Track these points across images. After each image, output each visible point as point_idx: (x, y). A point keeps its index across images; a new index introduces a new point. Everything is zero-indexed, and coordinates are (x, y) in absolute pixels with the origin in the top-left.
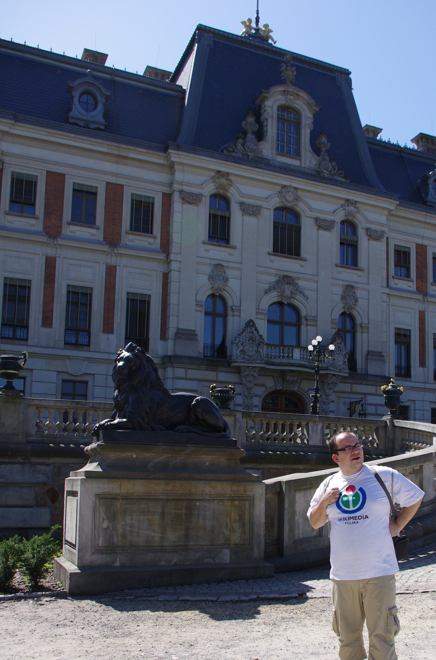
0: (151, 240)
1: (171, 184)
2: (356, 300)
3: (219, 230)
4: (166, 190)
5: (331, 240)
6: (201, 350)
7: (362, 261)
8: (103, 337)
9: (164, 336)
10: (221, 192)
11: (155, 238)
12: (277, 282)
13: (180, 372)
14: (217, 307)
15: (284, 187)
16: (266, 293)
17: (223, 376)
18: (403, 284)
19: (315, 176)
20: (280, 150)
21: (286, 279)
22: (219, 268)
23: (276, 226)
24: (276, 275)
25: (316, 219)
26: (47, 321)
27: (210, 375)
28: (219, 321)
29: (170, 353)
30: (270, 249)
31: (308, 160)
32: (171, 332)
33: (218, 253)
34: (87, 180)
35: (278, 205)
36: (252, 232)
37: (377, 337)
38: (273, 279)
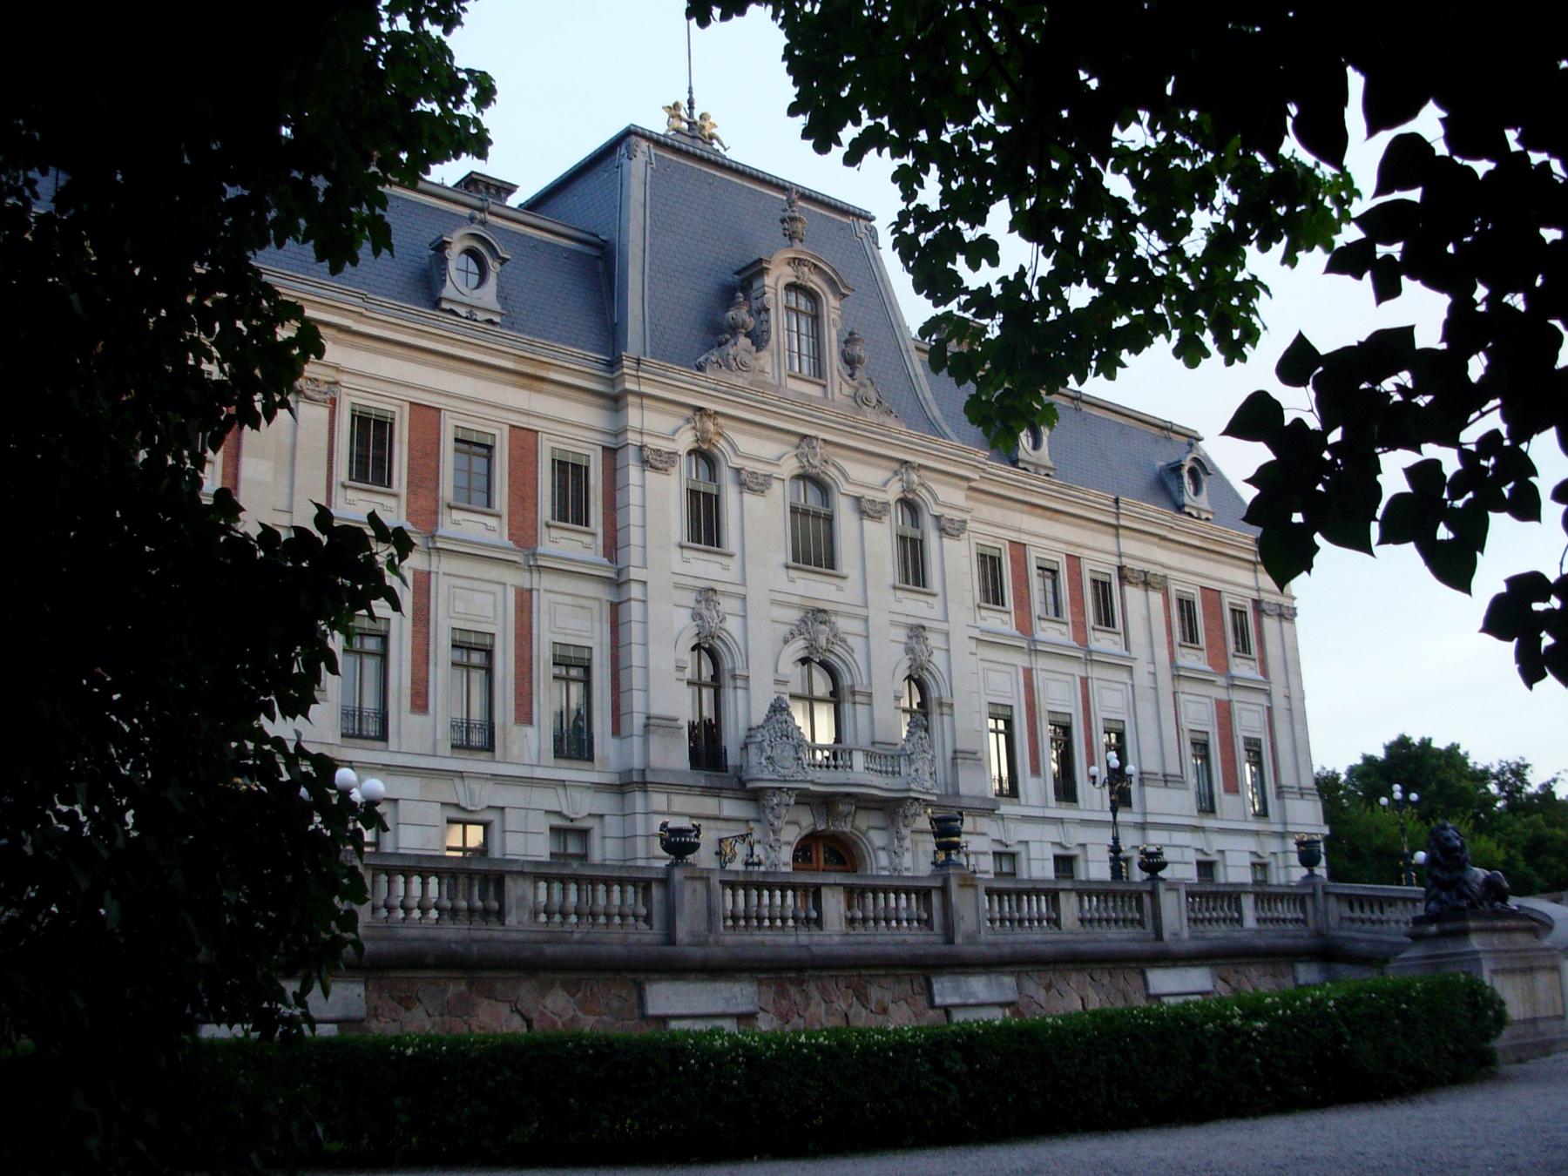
0: (588, 539)
1: (619, 432)
3: (705, 523)
4: (609, 441)
5: (881, 538)
8: (516, 731)
9: (616, 730)
10: (705, 447)
11: (593, 534)
12: (803, 621)
15: (804, 437)
16: (786, 642)
17: (730, 808)
21: (817, 615)
22: (708, 594)
24: (800, 607)
25: (858, 499)
28: (707, 694)
29: (637, 763)
35: (796, 472)
36: (759, 522)
38: (795, 615)
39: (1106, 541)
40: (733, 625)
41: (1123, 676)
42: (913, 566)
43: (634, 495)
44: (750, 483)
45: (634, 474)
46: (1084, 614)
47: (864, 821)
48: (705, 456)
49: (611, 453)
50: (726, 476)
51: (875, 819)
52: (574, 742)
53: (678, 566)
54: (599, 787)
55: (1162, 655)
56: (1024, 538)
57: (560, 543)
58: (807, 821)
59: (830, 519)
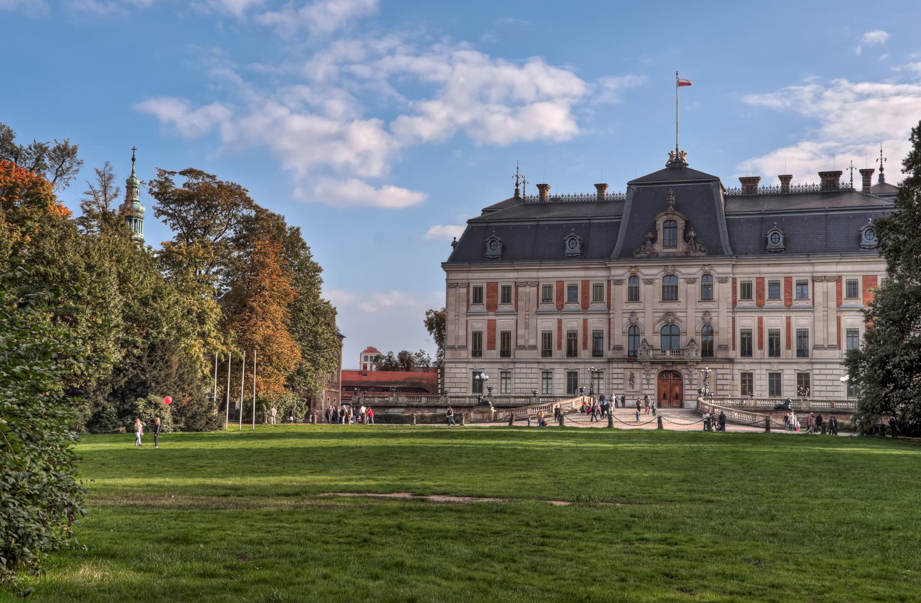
3: (634, 296)
7: (715, 297)
13: (615, 365)
14: (634, 331)
17: (635, 366)
18: (746, 304)
19: (685, 257)
20: (664, 247)
21: (668, 313)
22: (633, 313)
23: (663, 287)
27: (630, 365)
31: (682, 247)
32: (612, 347)
33: (633, 306)
38: (662, 314)
39: (809, 268)
40: (641, 320)
41: (811, 314)
42: (707, 295)
44: (649, 282)
45: (612, 287)
46: (791, 295)
47: (679, 368)
49: (609, 281)
50: (641, 282)
51: (684, 366)
52: (597, 353)
53: (625, 307)
55: (833, 304)
56: (762, 275)
57: (594, 306)
58: (660, 367)
59: (676, 287)
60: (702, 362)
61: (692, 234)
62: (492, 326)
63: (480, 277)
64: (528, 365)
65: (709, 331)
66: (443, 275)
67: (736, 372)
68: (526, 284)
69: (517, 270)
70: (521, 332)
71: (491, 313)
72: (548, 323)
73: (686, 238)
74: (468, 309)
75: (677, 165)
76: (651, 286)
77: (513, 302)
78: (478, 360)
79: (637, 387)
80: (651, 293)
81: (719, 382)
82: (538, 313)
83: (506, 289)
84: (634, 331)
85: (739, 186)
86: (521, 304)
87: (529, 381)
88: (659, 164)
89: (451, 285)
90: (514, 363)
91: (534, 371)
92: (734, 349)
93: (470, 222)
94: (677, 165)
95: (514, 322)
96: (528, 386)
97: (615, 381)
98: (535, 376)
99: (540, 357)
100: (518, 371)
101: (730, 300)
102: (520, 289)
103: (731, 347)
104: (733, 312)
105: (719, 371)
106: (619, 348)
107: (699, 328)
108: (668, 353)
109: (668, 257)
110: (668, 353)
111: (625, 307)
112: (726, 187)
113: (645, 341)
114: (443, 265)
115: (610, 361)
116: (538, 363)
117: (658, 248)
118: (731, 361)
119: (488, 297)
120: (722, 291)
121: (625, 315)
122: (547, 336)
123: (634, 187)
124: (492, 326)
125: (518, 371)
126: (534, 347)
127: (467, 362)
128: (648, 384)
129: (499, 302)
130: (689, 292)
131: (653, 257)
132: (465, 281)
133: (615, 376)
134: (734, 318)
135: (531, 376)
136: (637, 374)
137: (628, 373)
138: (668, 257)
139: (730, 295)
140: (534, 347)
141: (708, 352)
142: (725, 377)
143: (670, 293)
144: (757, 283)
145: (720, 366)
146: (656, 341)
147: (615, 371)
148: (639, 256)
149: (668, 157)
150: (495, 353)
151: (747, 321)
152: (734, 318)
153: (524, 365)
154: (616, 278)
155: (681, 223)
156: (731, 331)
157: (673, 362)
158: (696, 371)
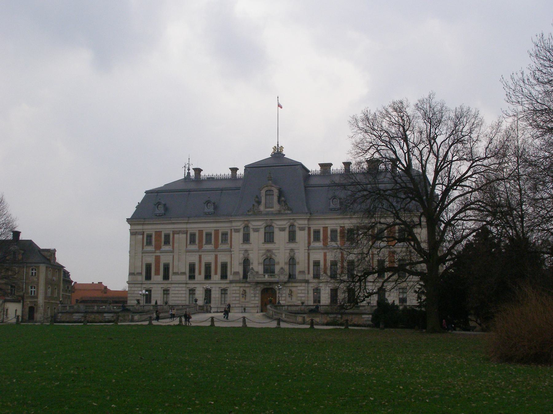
2: (294, 254)
3: (246, 239)
5: (285, 235)
6: (242, 277)
8: (215, 276)
13: (234, 285)
14: (246, 262)
17: (247, 285)
19: (279, 213)
20: (266, 207)
21: (268, 251)
22: (246, 251)
23: (265, 233)
25: (279, 228)
26: (200, 273)
27: (243, 285)
30: (263, 242)
31: (276, 207)
33: (246, 246)
34: (209, 231)
37: (301, 266)
38: (264, 251)
42: (292, 238)
43: (233, 237)
44: (256, 230)
45: (233, 233)
48: (246, 227)
49: (231, 230)
52: (224, 276)
54: (228, 283)
56: (326, 226)
57: (222, 247)
58: (262, 286)
59: (273, 233)
60: (288, 282)
61: (283, 199)
62: (158, 259)
63: (150, 229)
64: (181, 285)
65: (292, 262)
66: (128, 226)
67: (310, 288)
68: (179, 232)
69: (174, 223)
70: (176, 263)
71: (157, 251)
72: (194, 258)
73: (279, 201)
74: (143, 248)
75: (278, 154)
76: (257, 233)
77: (171, 244)
78: (149, 282)
79: (247, 300)
80: (257, 238)
81: (299, 295)
82: (187, 251)
83: (167, 236)
84: (246, 262)
85: (318, 168)
86: (176, 245)
87: (180, 295)
88: (267, 154)
89: (133, 233)
90: (172, 284)
91: (184, 289)
92: (309, 273)
93: (147, 192)
94: (278, 154)
95: (171, 257)
96: (180, 299)
97: (234, 295)
98: (184, 292)
99: (188, 279)
100: (173, 289)
101: (306, 242)
102: (176, 236)
103: (306, 272)
104: (308, 250)
105: (299, 288)
106: (236, 273)
107: (287, 260)
108: (266, 276)
109: (267, 214)
110: (266, 276)
111: (241, 246)
112: (310, 169)
113: (252, 269)
114: (128, 220)
115: (231, 282)
116: (186, 283)
117: (262, 208)
118: (307, 282)
119: (155, 241)
120: (301, 236)
121: (241, 252)
122: (192, 268)
123: (248, 169)
124: (158, 259)
125: (173, 289)
126: (184, 273)
127: (142, 284)
128: (255, 297)
129: (163, 243)
130: (281, 237)
131: (259, 213)
132: (142, 231)
133: (234, 292)
134: (309, 254)
135: (182, 292)
136: (247, 290)
137: (242, 289)
138: (267, 214)
139: (306, 238)
140: (184, 273)
141: (291, 277)
142: (303, 292)
143: (269, 238)
144: (324, 231)
145: (299, 284)
146: (260, 269)
147: (234, 288)
148: (250, 213)
149: (273, 150)
150: (160, 278)
151: (317, 256)
152: (309, 254)
153: (177, 285)
154: (235, 228)
155: (276, 192)
156: (307, 261)
157: (271, 283)
158: (285, 288)
